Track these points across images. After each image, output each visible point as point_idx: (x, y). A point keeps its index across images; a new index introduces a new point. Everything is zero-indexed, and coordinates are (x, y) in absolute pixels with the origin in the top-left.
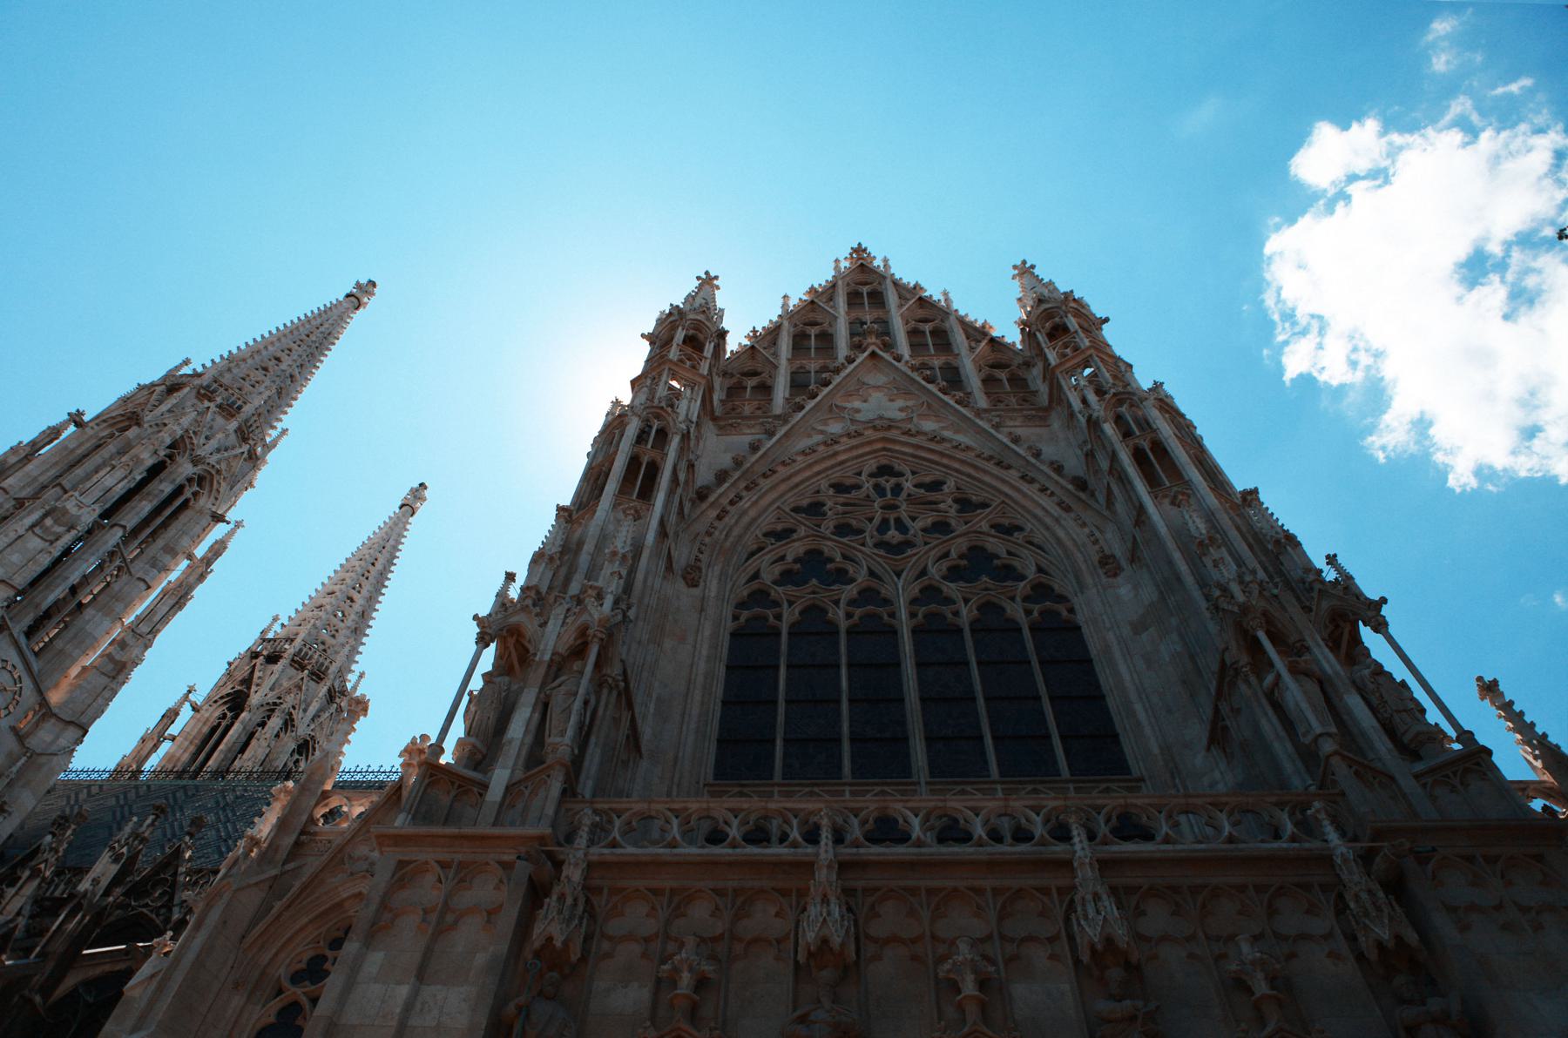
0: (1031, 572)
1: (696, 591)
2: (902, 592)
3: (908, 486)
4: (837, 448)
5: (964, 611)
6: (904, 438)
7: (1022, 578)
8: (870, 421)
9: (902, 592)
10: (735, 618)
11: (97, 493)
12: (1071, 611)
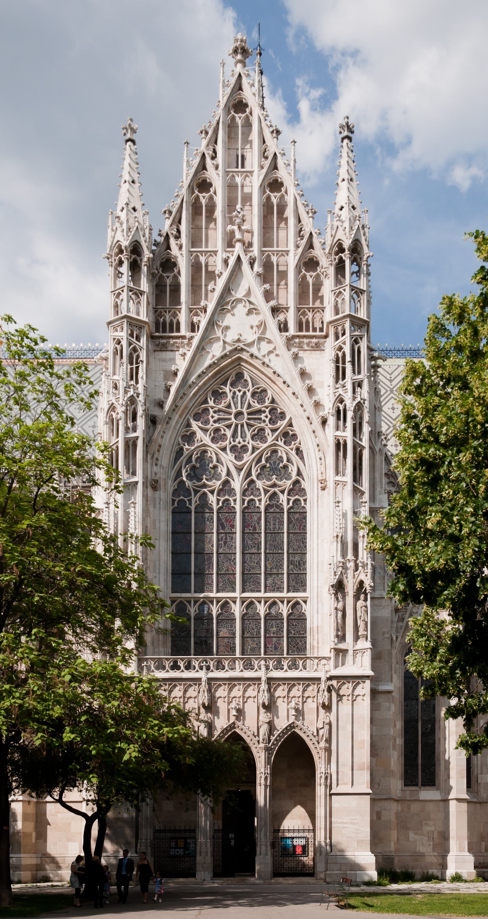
5: (263, 502)
7: (289, 478)
10: (173, 501)
12: (305, 500)
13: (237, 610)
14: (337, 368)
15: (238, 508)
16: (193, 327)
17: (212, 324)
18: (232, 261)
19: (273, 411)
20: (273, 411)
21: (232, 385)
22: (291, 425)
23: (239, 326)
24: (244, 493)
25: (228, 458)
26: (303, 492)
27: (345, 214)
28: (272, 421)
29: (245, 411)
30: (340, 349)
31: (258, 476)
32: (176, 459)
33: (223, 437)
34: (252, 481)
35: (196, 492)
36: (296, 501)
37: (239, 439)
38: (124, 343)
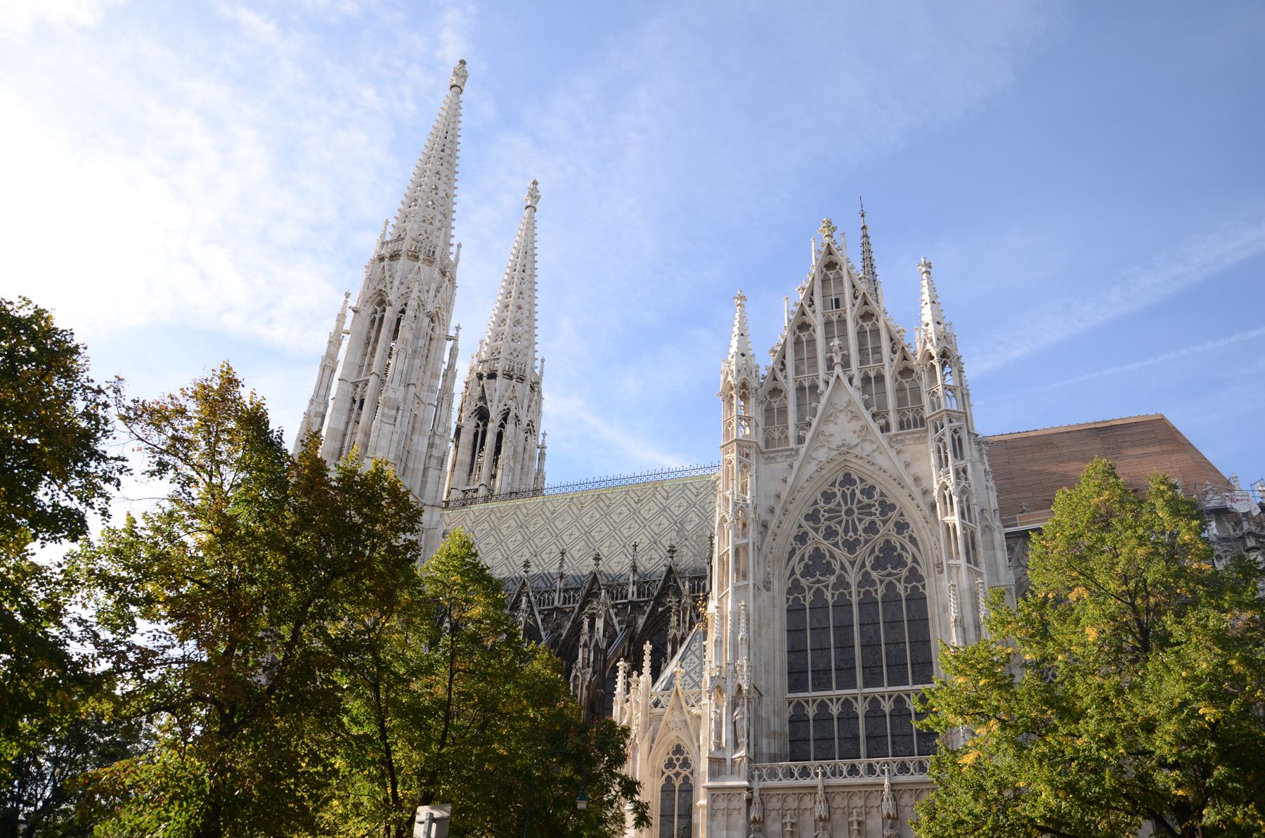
0: (909, 560)
1: (770, 594)
2: (853, 577)
3: (857, 492)
4: (824, 472)
6: (855, 460)
8: (839, 447)
9: (853, 577)
11: (397, 377)
12: (924, 586)
13: (861, 708)
14: (940, 457)
15: (855, 600)
16: (800, 440)
17: (818, 434)
18: (832, 381)
19: (882, 504)
20: (882, 504)
22: (902, 515)
23: (843, 430)
24: (860, 584)
25: (842, 554)
26: (921, 579)
27: (931, 328)
28: (883, 513)
29: (854, 507)
30: (941, 440)
31: (873, 568)
33: (836, 534)
34: (867, 573)
35: (810, 588)
36: (915, 588)
37: (851, 533)
38: (734, 462)
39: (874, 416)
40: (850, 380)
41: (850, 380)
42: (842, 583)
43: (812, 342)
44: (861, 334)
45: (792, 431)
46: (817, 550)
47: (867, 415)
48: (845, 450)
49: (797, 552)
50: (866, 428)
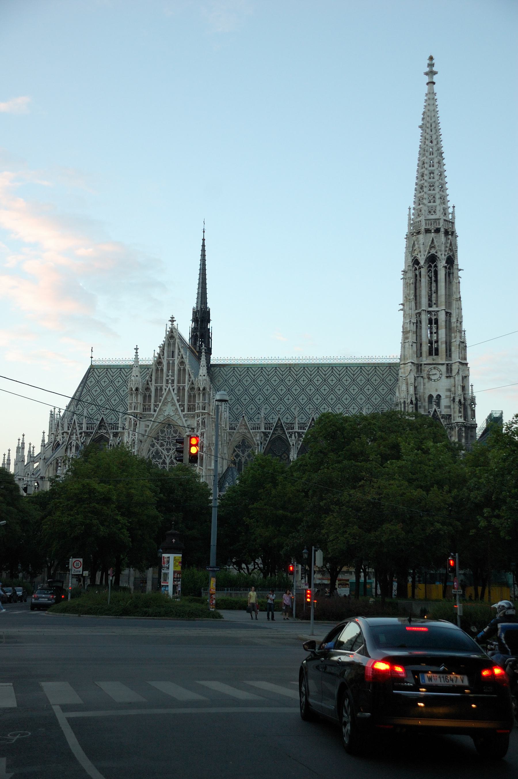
2: (168, 461)
9: (168, 461)
17: (160, 409)
18: (167, 389)
21: (167, 428)
25: (165, 452)
32: (148, 452)
33: (164, 445)
39: (180, 405)
40: (174, 390)
41: (174, 390)
42: (164, 462)
43: (162, 370)
44: (179, 370)
45: (152, 407)
46: (157, 450)
47: (177, 404)
48: (169, 417)
49: (151, 451)
50: (177, 409)
